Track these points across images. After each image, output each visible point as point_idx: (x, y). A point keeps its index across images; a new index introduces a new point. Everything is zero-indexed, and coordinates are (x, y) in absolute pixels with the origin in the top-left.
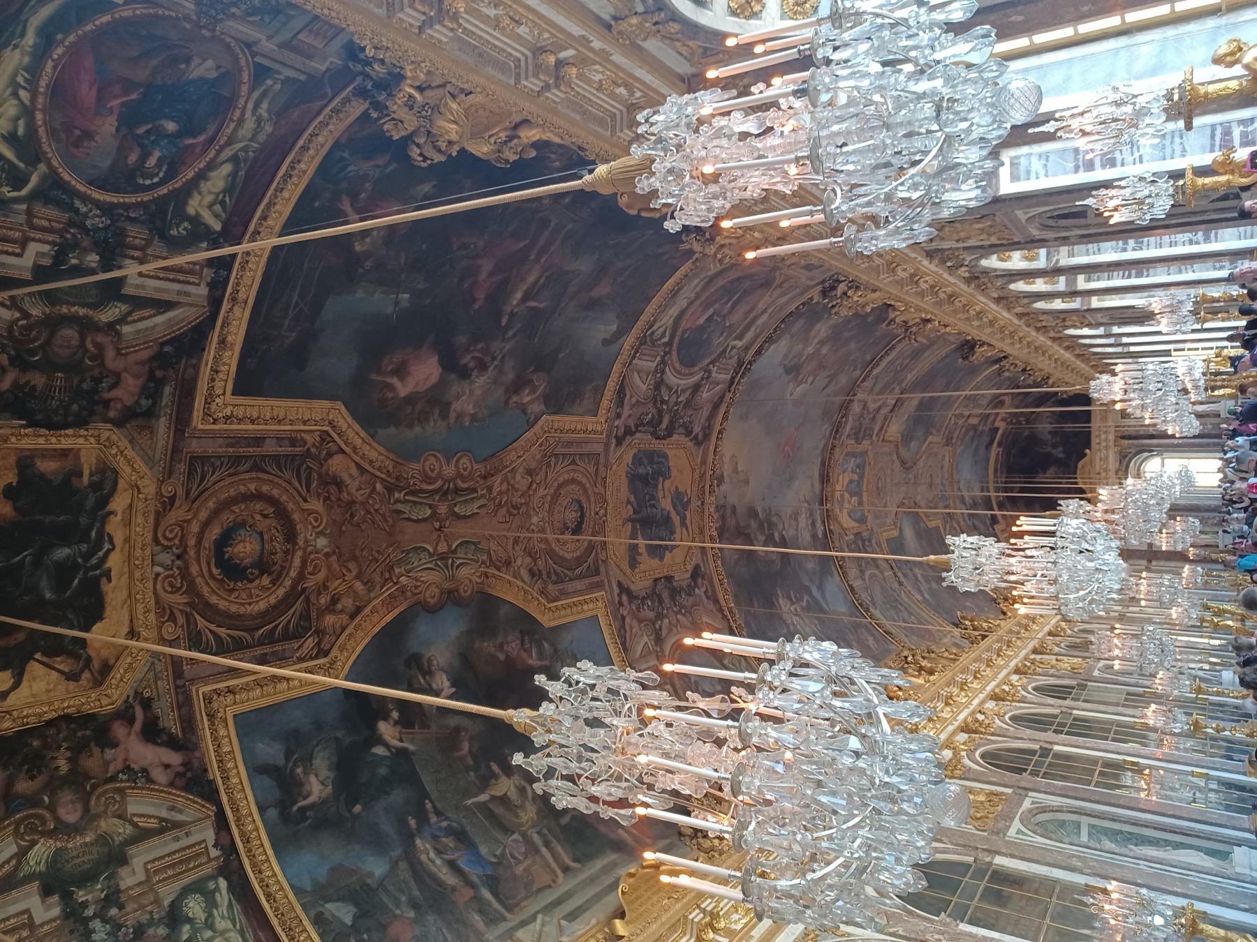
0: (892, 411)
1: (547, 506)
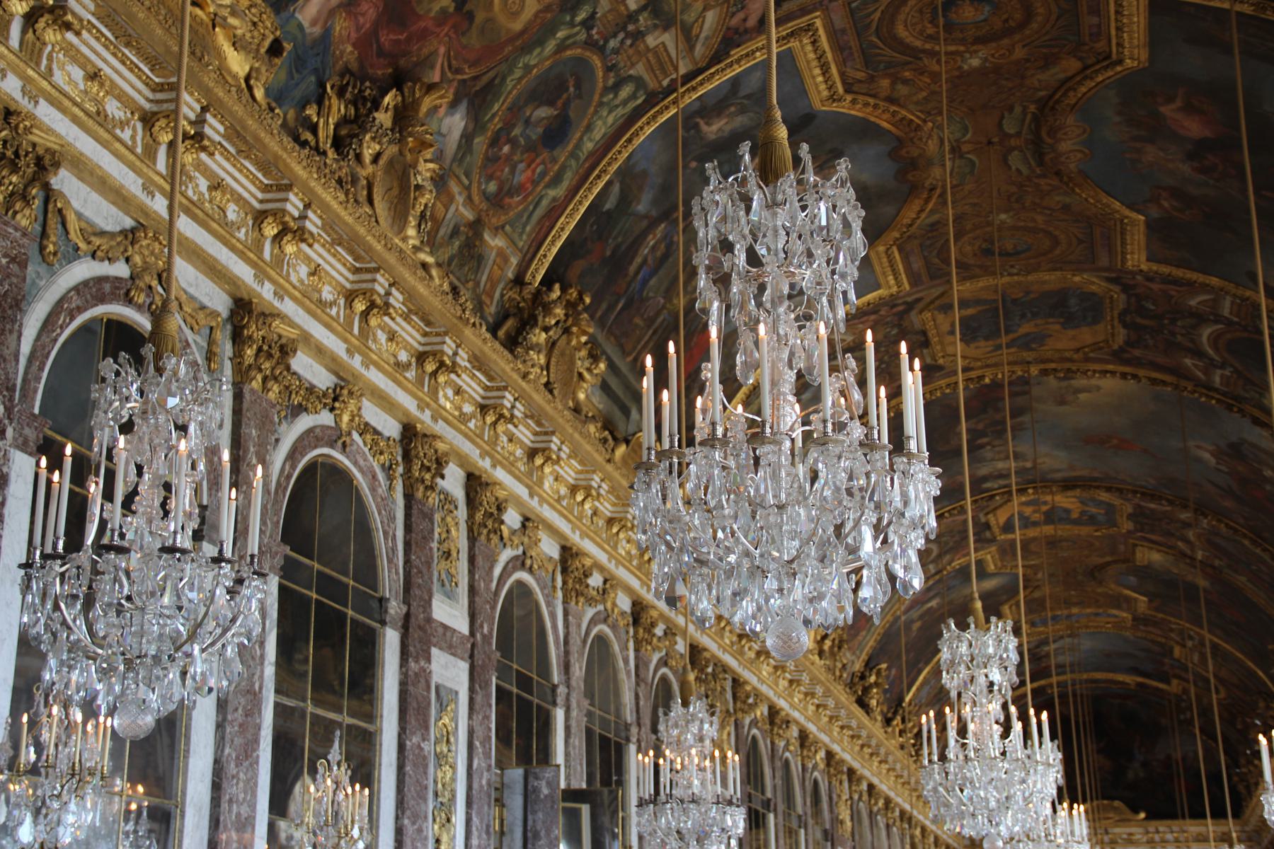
0: (1184, 555)
1: (1022, 224)
